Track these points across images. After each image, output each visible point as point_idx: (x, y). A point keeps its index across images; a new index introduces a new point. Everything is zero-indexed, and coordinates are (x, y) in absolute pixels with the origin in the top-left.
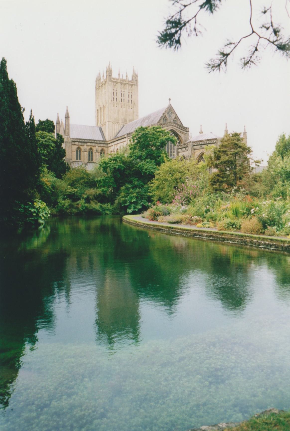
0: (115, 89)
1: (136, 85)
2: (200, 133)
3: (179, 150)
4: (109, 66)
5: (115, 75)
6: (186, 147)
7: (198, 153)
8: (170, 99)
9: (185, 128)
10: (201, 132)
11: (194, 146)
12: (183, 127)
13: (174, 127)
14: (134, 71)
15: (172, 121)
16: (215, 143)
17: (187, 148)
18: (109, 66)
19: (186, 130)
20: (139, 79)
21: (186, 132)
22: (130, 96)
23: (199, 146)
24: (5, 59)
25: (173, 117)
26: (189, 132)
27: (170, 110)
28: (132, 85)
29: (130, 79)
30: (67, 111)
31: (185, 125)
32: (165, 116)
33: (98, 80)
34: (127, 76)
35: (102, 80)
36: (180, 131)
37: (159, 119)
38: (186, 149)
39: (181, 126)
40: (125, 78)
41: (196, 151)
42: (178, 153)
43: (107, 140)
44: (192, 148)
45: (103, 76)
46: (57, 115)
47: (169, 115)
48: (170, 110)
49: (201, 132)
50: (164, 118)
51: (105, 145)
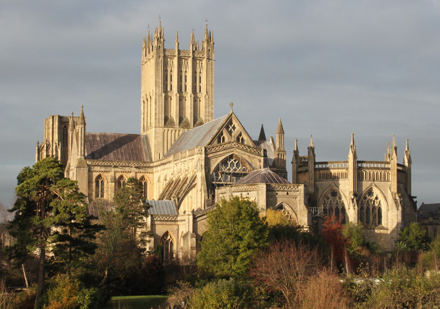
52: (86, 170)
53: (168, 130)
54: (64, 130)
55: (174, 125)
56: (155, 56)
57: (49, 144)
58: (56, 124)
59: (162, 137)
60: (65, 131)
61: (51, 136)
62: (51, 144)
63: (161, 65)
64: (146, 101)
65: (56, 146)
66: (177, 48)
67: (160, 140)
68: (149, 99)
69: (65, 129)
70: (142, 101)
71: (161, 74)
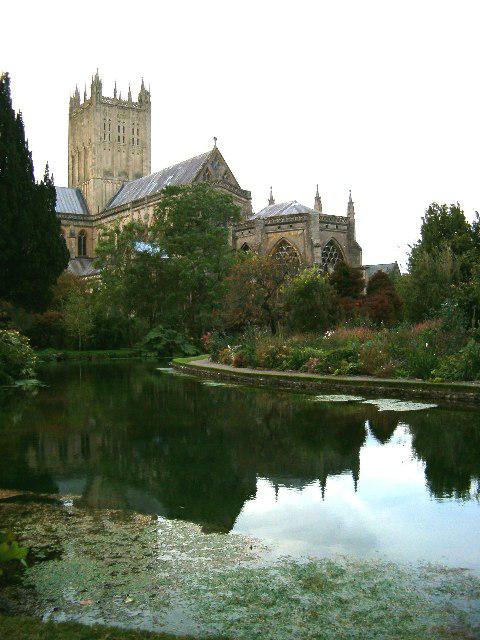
1: (148, 111)
3: (237, 234)
4: (97, 77)
5: (107, 92)
7: (274, 238)
10: (271, 201)
14: (142, 86)
15: (220, 178)
18: (97, 77)
19: (246, 195)
20: (152, 100)
22: (135, 130)
24: (9, 76)
25: (223, 172)
27: (216, 156)
28: (138, 111)
29: (135, 99)
30: (318, 194)
31: (243, 188)
32: (207, 170)
33: (74, 102)
34: (129, 94)
35: (82, 102)
40: (125, 98)
42: (235, 239)
45: (85, 95)
48: (216, 156)
49: (271, 201)
51: (88, 224)
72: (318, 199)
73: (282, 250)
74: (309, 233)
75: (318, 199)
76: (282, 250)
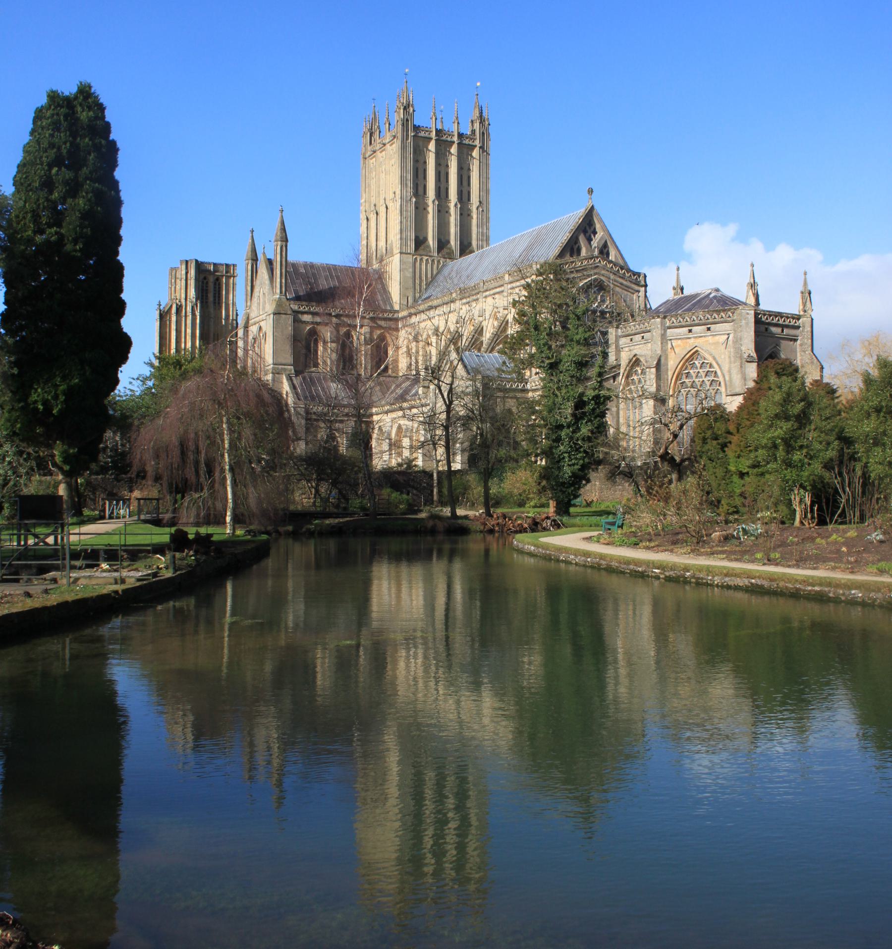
0: (422, 162)
2: (674, 289)
3: (623, 341)
6: (644, 332)
8: (591, 191)
9: (635, 274)
11: (669, 328)
12: (629, 270)
13: (603, 272)
15: (596, 253)
16: (733, 321)
17: (646, 335)
19: (638, 280)
21: (636, 288)
23: (686, 329)
26: (646, 286)
36: (621, 284)
37: (555, 250)
38: (643, 337)
39: (622, 268)
41: (675, 343)
42: (618, 350)
43: (397, 307)
44: (663, 336)
46: (251, 235)
47: (587, 235)
50: (571, 248)
52: (290, 319)
53: (421, 260)
54: (203, 282)
55: (430, 252)
56: (399, 135)
57: (181, 306)
58: (192, 272)
59: (411, 270)
60: (205, 285)
61: (183, 291)
62: (184, 304)
63: (410, 150)
64: (373, 217)
65: (193, 307)
66: (434, 125)
67: (409, 274)
68: (382, 210)
69: (205, 281)
70: (363, 216)
71: (410, 165)
72: (753, 285)
73: (693, 366)
74: (738, 341)
75: (753, 285)
76: (693, 366)
